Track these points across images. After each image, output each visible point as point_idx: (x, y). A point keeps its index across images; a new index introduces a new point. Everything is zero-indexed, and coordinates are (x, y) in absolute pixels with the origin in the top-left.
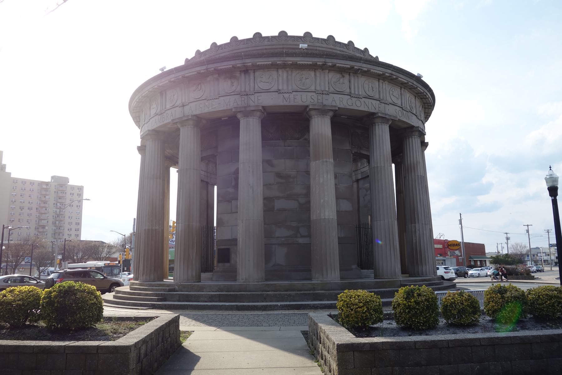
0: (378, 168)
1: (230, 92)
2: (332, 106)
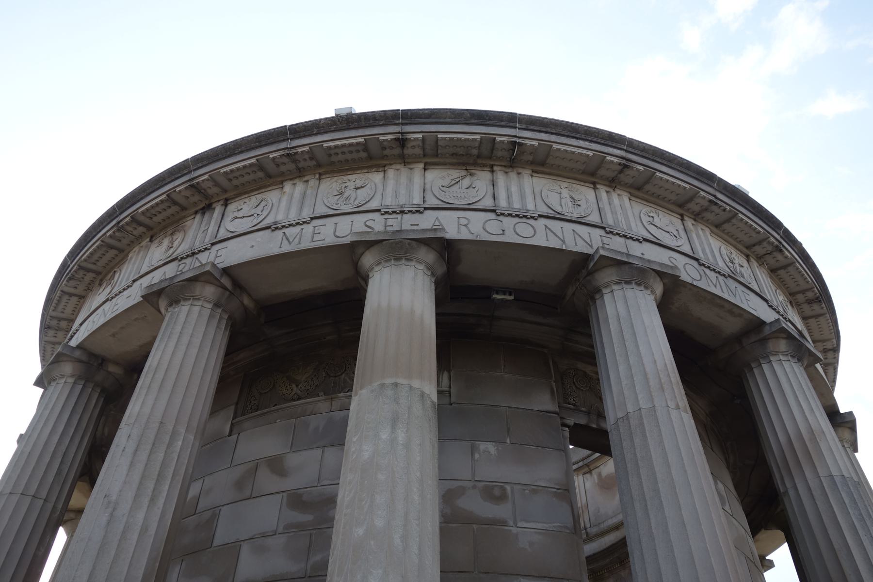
0: (628, 419)
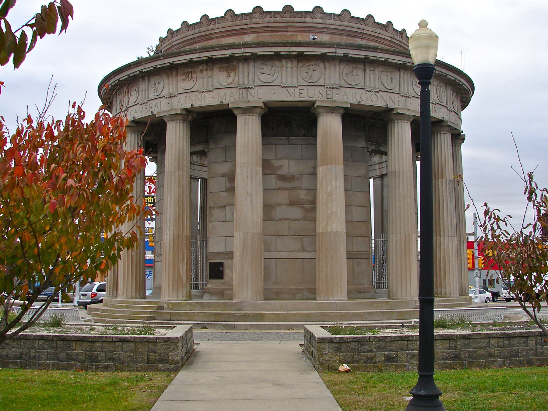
0: (395, 173)
1: (226, 84)
2: (342, 102)
